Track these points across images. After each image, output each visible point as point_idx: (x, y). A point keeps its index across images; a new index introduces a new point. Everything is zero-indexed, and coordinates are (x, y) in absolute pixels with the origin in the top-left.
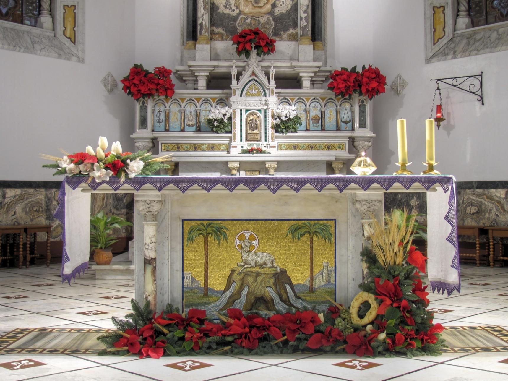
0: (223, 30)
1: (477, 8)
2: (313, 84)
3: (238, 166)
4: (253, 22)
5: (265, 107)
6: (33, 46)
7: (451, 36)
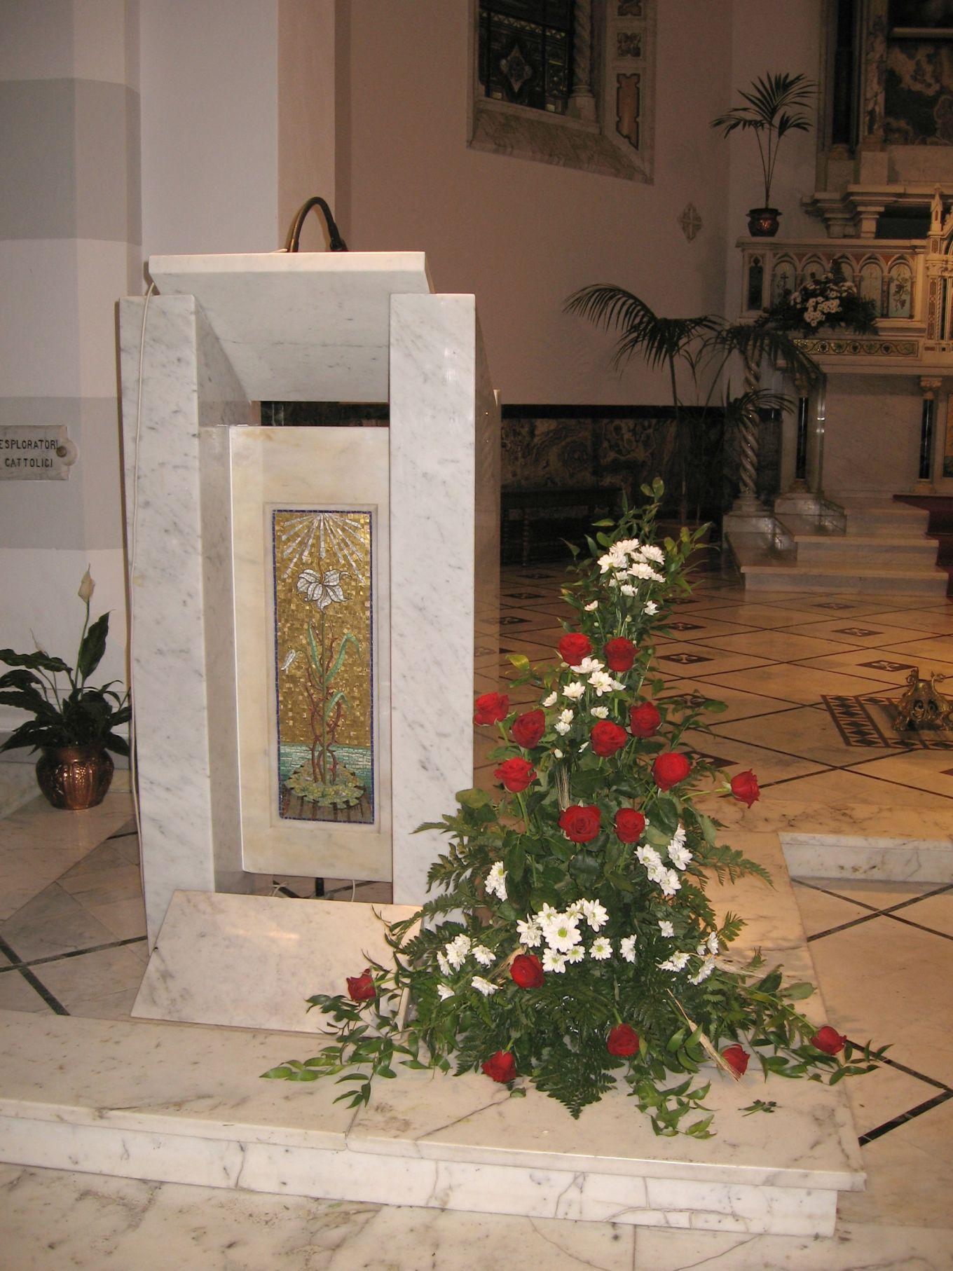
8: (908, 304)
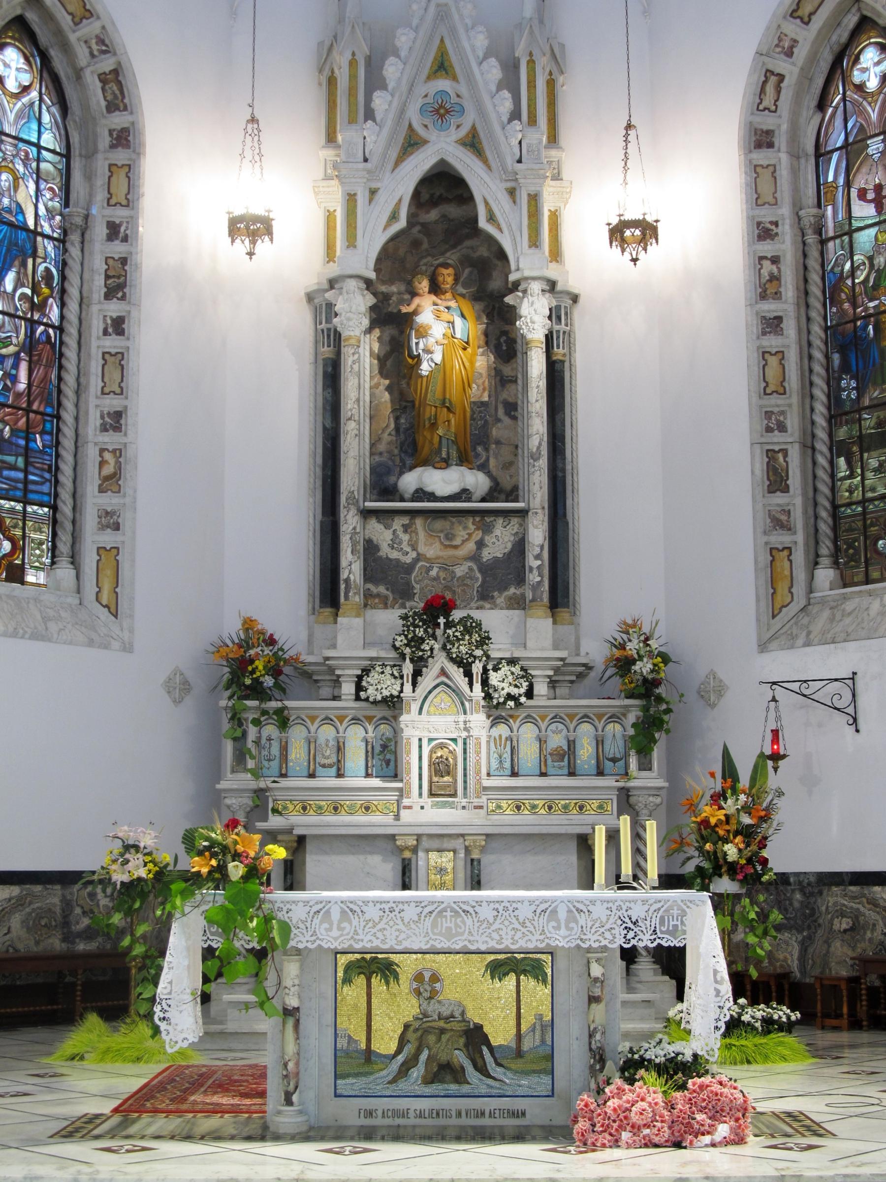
0: (387, 589)
1: (851, 551)
2: (554, 688)
3: (415, 842)
4: (442, 575)
5: (464, 734)
6: (45, 624)
7: (803, 602)
8: (392, 764)
